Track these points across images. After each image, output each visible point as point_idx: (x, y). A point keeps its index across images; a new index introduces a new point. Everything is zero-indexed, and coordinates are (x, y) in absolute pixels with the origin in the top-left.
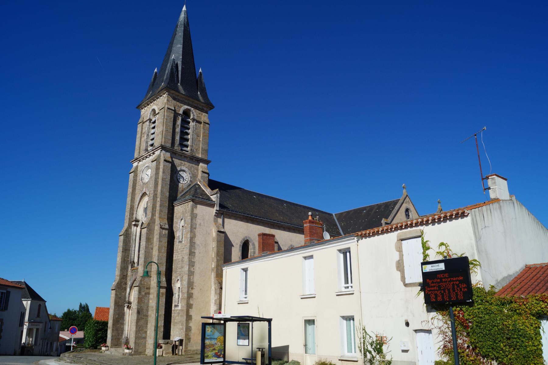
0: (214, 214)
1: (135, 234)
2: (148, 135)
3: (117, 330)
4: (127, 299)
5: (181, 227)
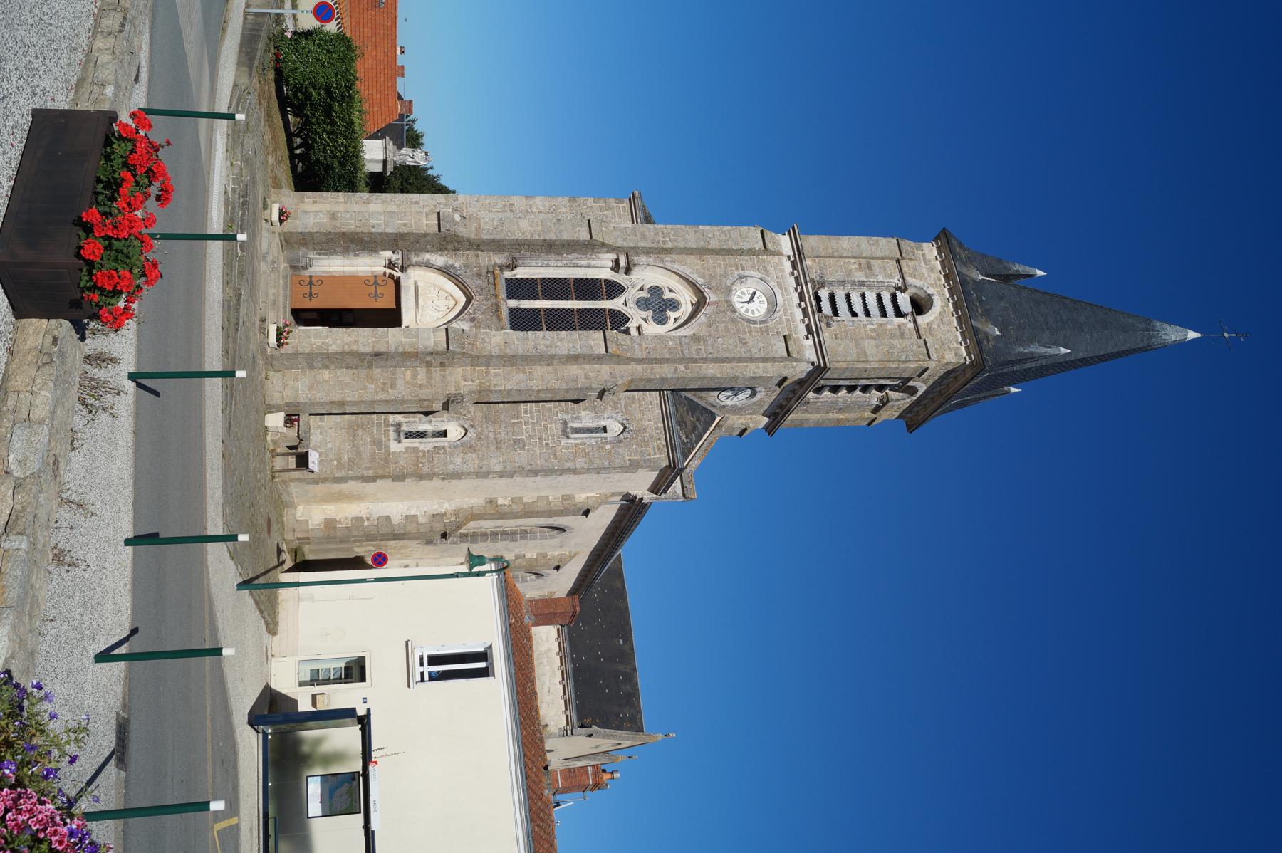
0: (633, 493)
1: (594, 263)
2: (862, 284)
3: (329, 241)
4: (414, 259)
5: (602, 423)
